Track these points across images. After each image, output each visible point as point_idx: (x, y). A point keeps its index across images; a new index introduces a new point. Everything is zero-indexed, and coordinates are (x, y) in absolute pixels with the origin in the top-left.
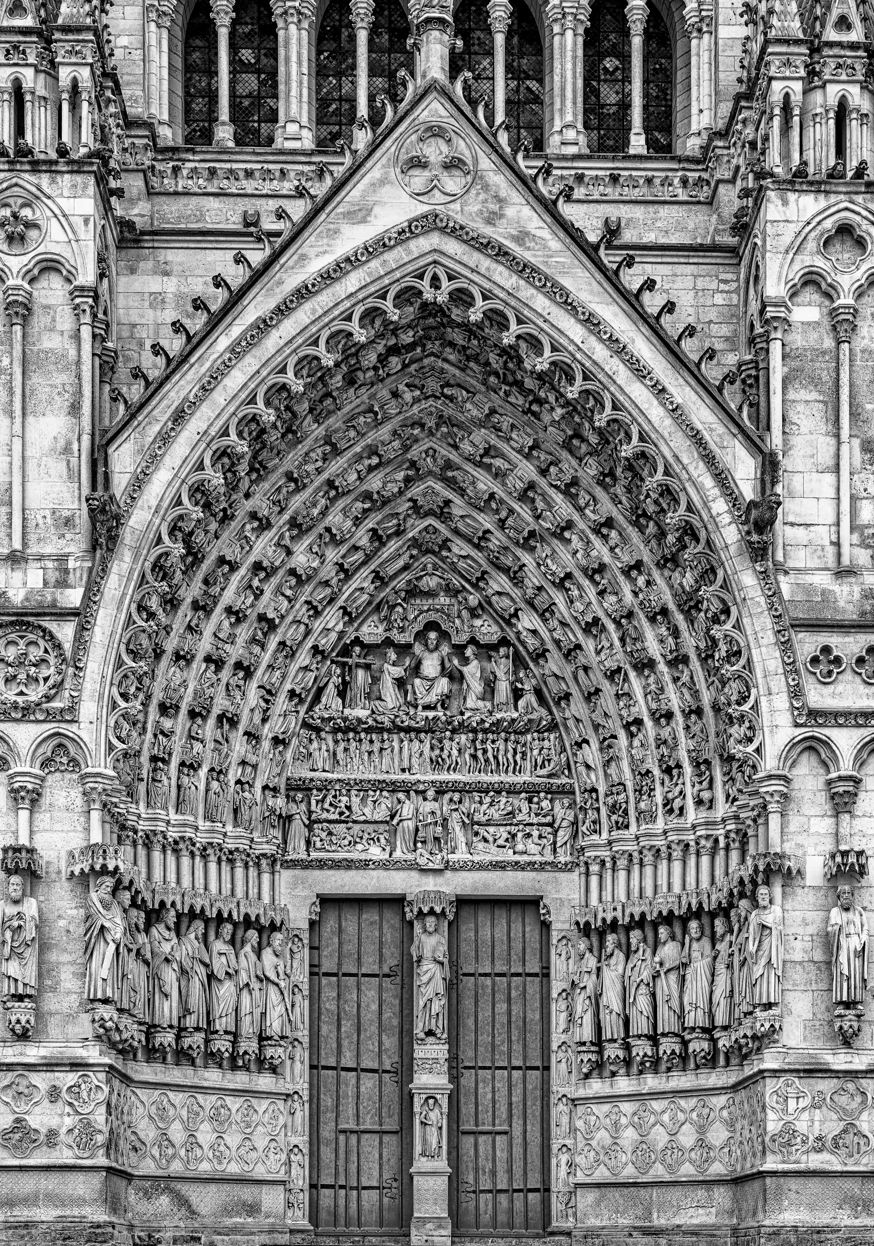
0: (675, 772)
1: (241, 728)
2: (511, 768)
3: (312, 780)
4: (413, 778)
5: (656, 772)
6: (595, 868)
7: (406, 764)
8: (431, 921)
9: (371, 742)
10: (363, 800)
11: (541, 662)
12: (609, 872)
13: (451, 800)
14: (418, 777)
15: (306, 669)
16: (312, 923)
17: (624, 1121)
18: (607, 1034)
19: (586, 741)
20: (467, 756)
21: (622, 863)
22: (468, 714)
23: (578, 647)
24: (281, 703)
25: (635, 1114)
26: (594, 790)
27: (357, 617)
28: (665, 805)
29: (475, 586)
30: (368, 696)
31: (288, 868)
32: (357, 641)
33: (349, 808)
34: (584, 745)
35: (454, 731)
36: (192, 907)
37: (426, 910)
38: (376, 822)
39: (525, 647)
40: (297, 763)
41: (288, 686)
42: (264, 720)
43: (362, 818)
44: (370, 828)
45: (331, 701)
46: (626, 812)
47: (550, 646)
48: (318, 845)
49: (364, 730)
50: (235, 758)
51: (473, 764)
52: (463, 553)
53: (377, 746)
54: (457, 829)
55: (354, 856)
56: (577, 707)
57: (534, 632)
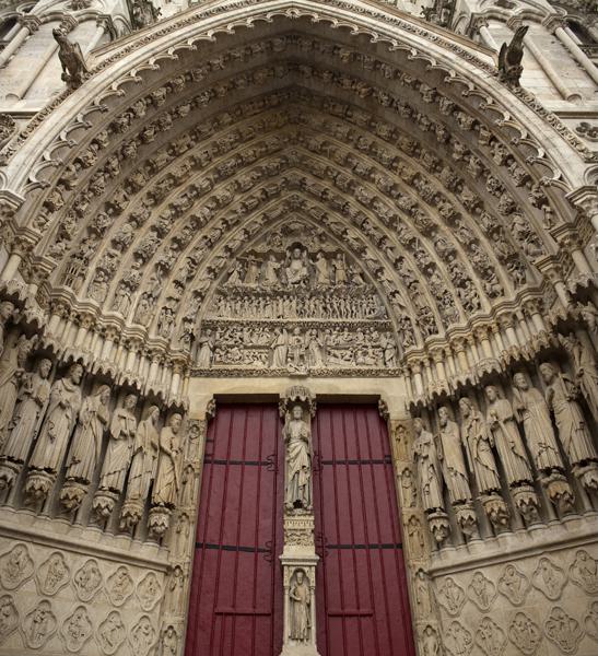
4: (285, 321)
6: (416, 369)
7: (280, 313)
8: (298, 411)
10: (251, 335)
12: (428, 370)
13: (311, 335)
15: (219, 257)
17: (490, 590)
18: (455, 496)
21: (438, 357)
23: (385, 237)
24: (202, 273)
25: (501, 580)
26: (407, 319)
27: (255, 236)
29: (321, 223)
30: (257, 279)
31: (196, 376)
32: (253, 252)
33: (241, 339)
35: (311, 297)
37: (293, 399)
38: (260, 347)
39: (352, 250)
41: (208, 265)
42: (190, 279)
45: (234, 279)
46: (434, 322)
48: (218, 359)
49: (255, 295)
53: (262, 303)
54: (316, 350)
55: (243, 367)
56: (389, 274)
57: (357, 239)
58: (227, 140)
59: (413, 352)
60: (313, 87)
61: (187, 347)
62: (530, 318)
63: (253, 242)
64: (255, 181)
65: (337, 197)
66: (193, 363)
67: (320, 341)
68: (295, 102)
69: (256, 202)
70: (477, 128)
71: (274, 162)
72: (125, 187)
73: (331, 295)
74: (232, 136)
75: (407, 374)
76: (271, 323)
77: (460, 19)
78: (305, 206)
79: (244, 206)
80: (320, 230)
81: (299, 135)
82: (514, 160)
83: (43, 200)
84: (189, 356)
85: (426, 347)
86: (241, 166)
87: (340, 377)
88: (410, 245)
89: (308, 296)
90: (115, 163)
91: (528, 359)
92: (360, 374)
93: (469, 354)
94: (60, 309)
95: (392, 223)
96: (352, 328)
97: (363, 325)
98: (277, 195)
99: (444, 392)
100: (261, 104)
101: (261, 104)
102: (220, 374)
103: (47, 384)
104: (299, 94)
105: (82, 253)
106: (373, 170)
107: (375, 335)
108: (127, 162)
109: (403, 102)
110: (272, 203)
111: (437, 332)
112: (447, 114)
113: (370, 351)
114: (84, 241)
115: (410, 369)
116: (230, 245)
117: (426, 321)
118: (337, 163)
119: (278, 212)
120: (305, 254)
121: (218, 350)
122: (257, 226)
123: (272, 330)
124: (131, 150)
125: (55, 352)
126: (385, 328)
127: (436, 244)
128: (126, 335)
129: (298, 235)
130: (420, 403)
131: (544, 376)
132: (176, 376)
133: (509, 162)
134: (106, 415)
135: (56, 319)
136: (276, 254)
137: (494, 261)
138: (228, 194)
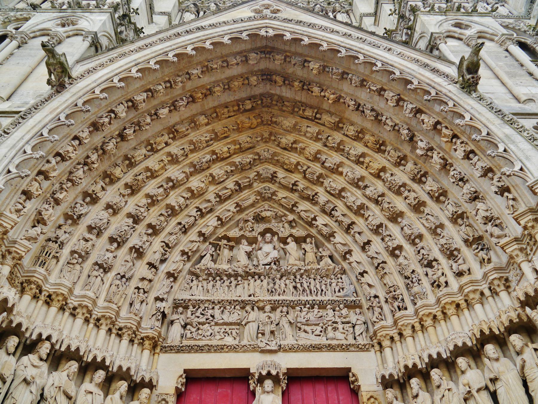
0: (434, 263)
1: (146, 259)
2: (320, 292)
3: (190, 300)
4: (256, 299)
5: (420, 271)
7: (252, 292)
9: (231, 283)
11: (332, 239)
14: (260, 298)
15: (193, 242)
16: (180, 395)
19: (366, 272)
20: (291, 288)
22: (289, 267)
24: (175, 256)
26: (376, 297)
28: (432, 284)
29: (292, 211)
30: (230, 261)
32: (226, 237)
34: (365, 274)
35: (282, 277)
36: (69, 346)
39: (322, 235)
40: (182, 292)
41: (181, 248)
42: (163, 261)
43: (221, 321)
44: (228, 328)
45: (207, 262)
46: (403, 300)
47: (336, 230)
48: (189, 335)
49: (226, 275)
50: (138, 276)
51: (295, 292)
52: (284, 196)
54: (287, 326)
55: (214, 342)
56: (357, 255)
57: (325, 225)
58: (203, 139)
59: (383, 327)
60: (284, 94)
61: (158, 324)
62: (497, 294)
63: (225, 228)
64: (229, 174)
65: (307, 188)
66: (164, 339)
67: (291, 317)
68: (268, 106)
69: (228, 192)
70: (439, 127)
71: (248, 158)
72: (104, 178)
73: (301, 275)
74: (208, 135)
75: (377, 347)
76: (243, 301)
77: (421, 38)
78: (277, 196)
79: (218, 196)
80: (291, 217)
81: (271, 134)
82: (476, 155)
83: (22, 189)
84: (160, 333)
85: (395, 322)
86: (214, 161)
87: (310, 351)
88: (377, 230)
89: (278, 276)
90: (94, 157)
91: (497, 332)
92: (331, 348)
93: (438, 328)
94: (31, 289)
95: (360, 211)
96: (322, 306)
97: (333, 302)
98: (250, 186)
99: (415, 365)
100: (236, 108)
101: (236, 108)
102: (191, 349)
103: (12, 360)
104: (271, 99)
105: (57, 238)
106: (341, 164)
107: (345, 311)
108: (106, 157)
109: (369, 106)
110: (245, 193)
111: (406, 309)
112: (411, 115)
113: (340, 326)
114: (60, 227)
115: (380, 344)
116: (203, 231)
117: (395, 298)
118: (307, 159)
119: (250, 201)
120: (275, 239)
121: (188, 327)
122: (231, 213)
123: (243, 308)
124: (110, 146)
125: (23, 329)
126: (353, 306)
127: (402, 229)
128: (97, 313)
129: (269, 222)
130: (391, 375)
131: (514, 347)
132: (147, 352)
133: (471, 156)
134: (72, 390)
135: (27, 298)
136: (247, 239)
137: (459, 243)
138: (202, 185)
